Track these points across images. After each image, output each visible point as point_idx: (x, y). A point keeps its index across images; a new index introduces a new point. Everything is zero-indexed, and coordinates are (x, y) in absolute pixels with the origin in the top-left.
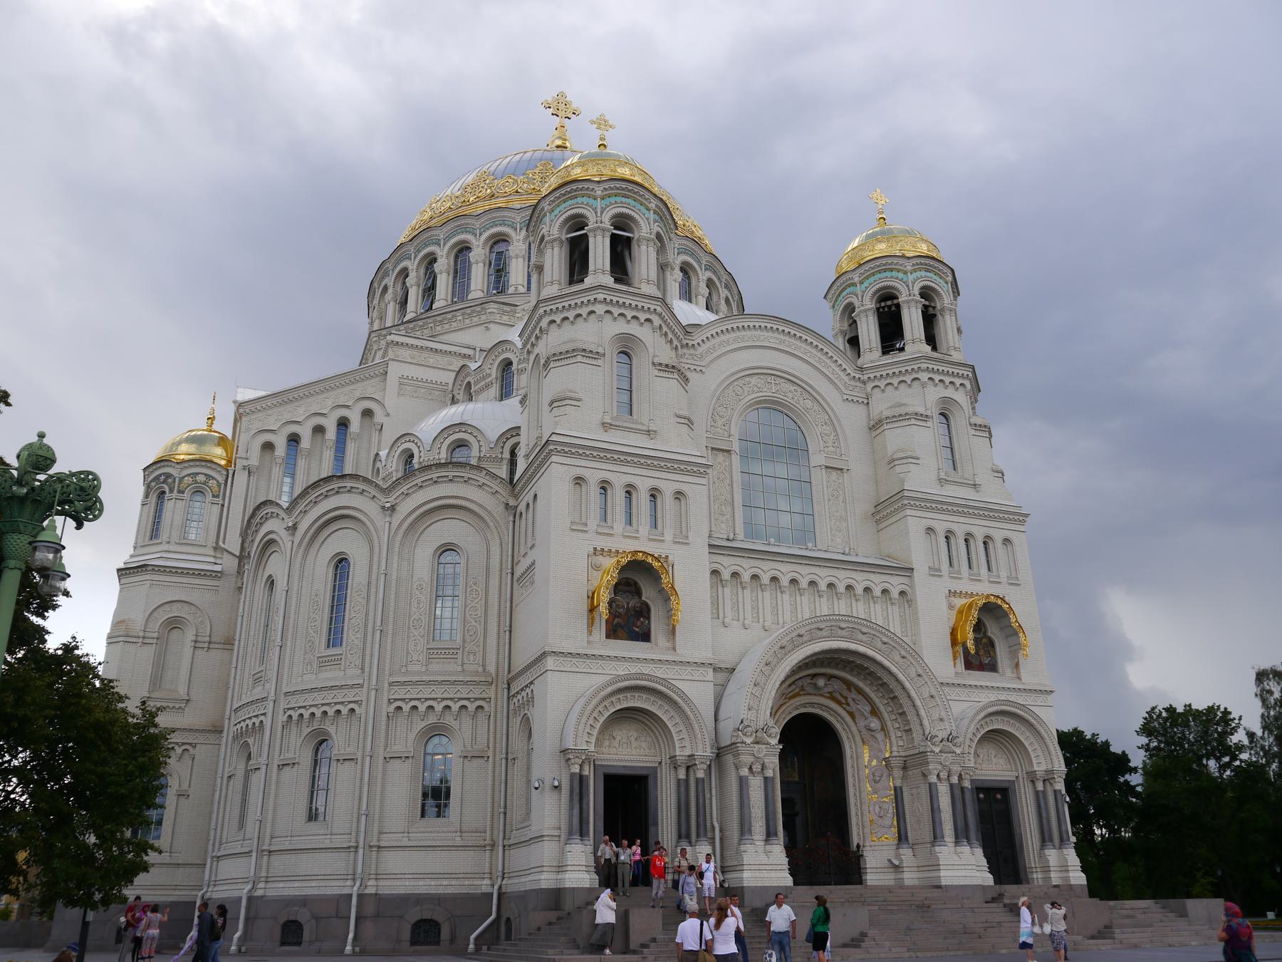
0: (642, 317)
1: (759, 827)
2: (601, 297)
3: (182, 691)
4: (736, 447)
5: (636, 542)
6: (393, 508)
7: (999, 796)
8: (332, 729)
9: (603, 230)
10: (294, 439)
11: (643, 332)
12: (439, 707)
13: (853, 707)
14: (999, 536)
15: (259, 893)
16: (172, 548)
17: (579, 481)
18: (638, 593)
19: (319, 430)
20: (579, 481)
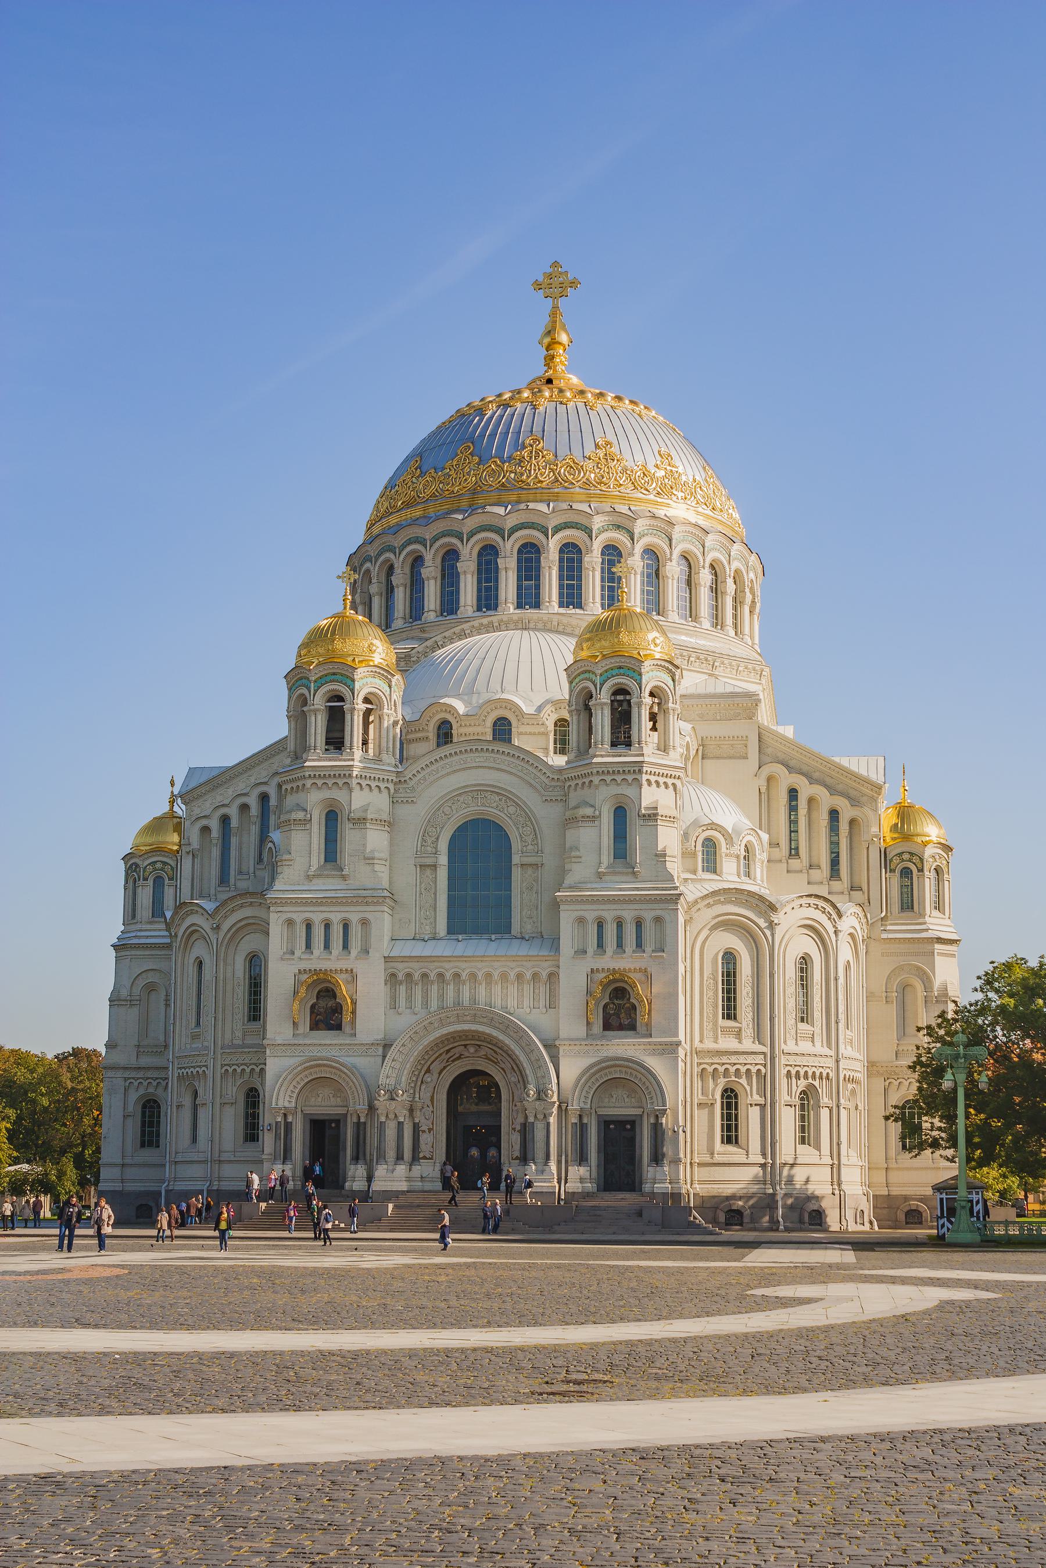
0: (340, 782)
1: (391, 1154)
2: (307, 774)
3: (162, 1038)
4: (443, 860)
5: (329, 962)
6: (218, 927)
7: (628, 1127)
8: (196, 1084)
9: (315, 711)
10: (225, 820)
11: (340, 795)
12: (248, 1070)
13: (503, 1066)
14: (648, 916)
15: (171, 1188)
16: (144, 927)
17: (290, 923)
18: (334, 996)
19: (244, 808)
20: (290, 923)
